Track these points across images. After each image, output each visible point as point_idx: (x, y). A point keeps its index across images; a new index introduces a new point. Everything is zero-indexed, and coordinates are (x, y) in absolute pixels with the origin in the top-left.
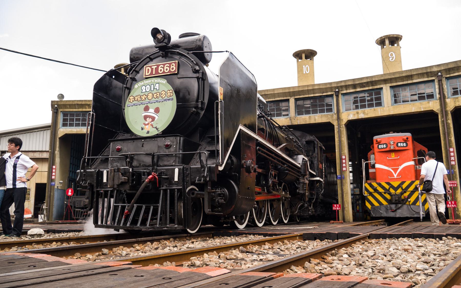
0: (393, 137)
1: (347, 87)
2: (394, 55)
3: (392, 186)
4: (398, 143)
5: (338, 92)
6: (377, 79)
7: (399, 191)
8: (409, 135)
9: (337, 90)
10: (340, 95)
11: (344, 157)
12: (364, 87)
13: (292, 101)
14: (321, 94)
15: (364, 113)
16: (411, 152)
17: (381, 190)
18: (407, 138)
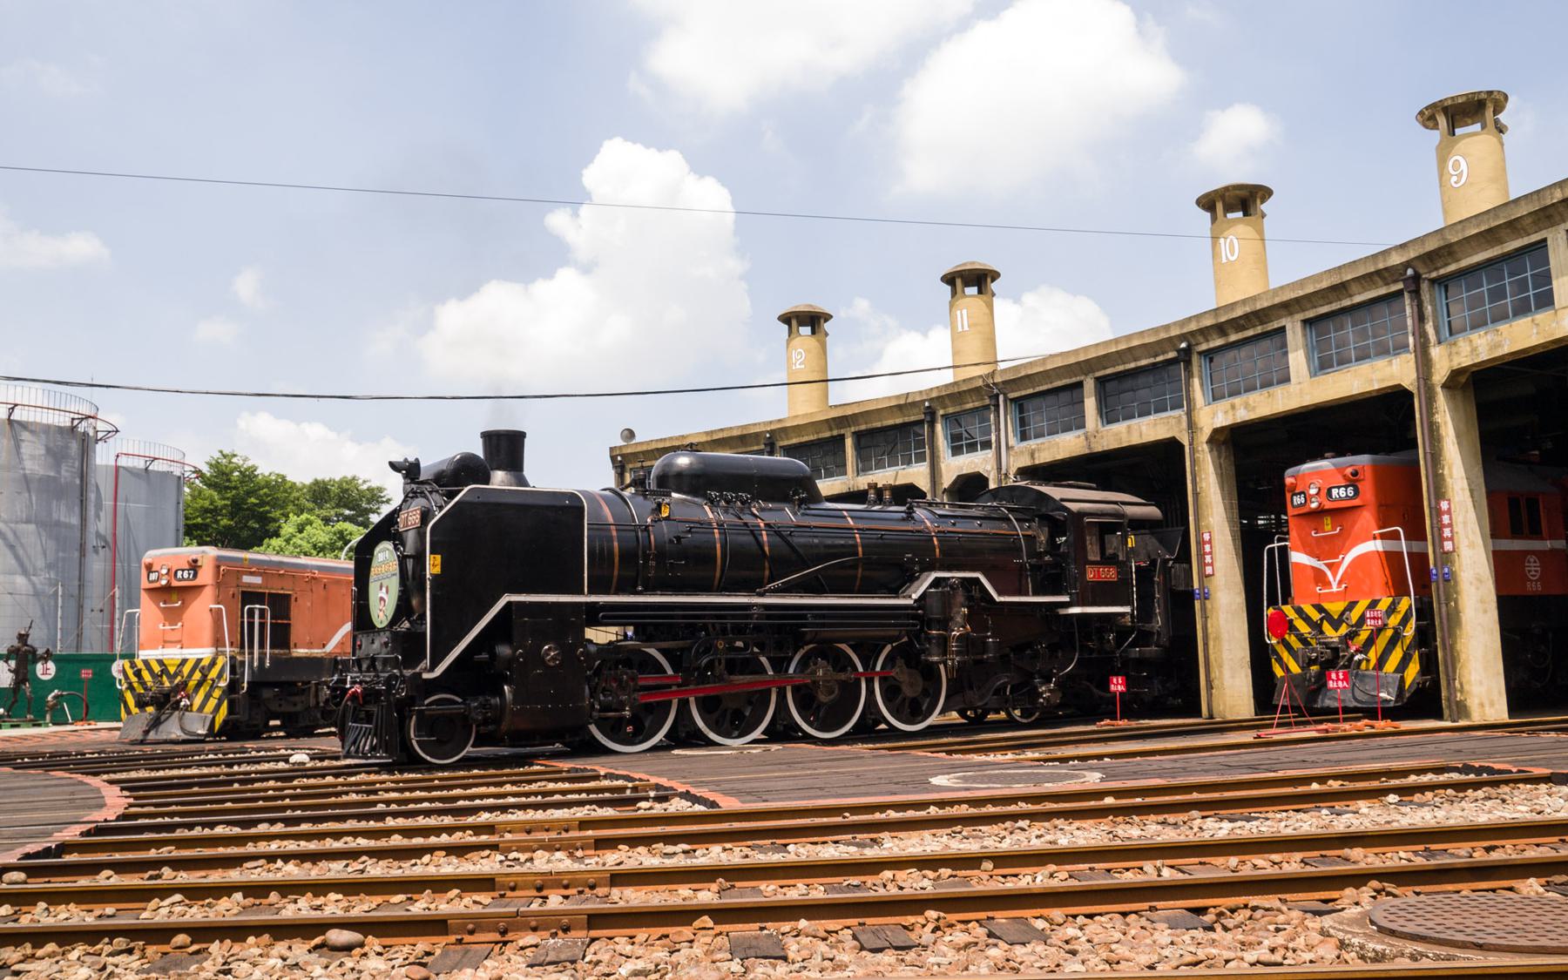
0: (1319, 473)
1: (1204, 332)
2: (1464, 166)
3: (1327, 616)
4: (1329, 490)
5: (1188, 352)
6: (1266, 305)
7: (1343, 630)
8: (1363, 460)
9: (1183, 345)
10: (1195, 358)
11: (1206, 537)
12: (1244, 328)
13: (1089, 385)
14: (1152, 360)
15: (1246, 406)
16: (1367, 518)
17: (1303, 628)
18: (1355, 474)
